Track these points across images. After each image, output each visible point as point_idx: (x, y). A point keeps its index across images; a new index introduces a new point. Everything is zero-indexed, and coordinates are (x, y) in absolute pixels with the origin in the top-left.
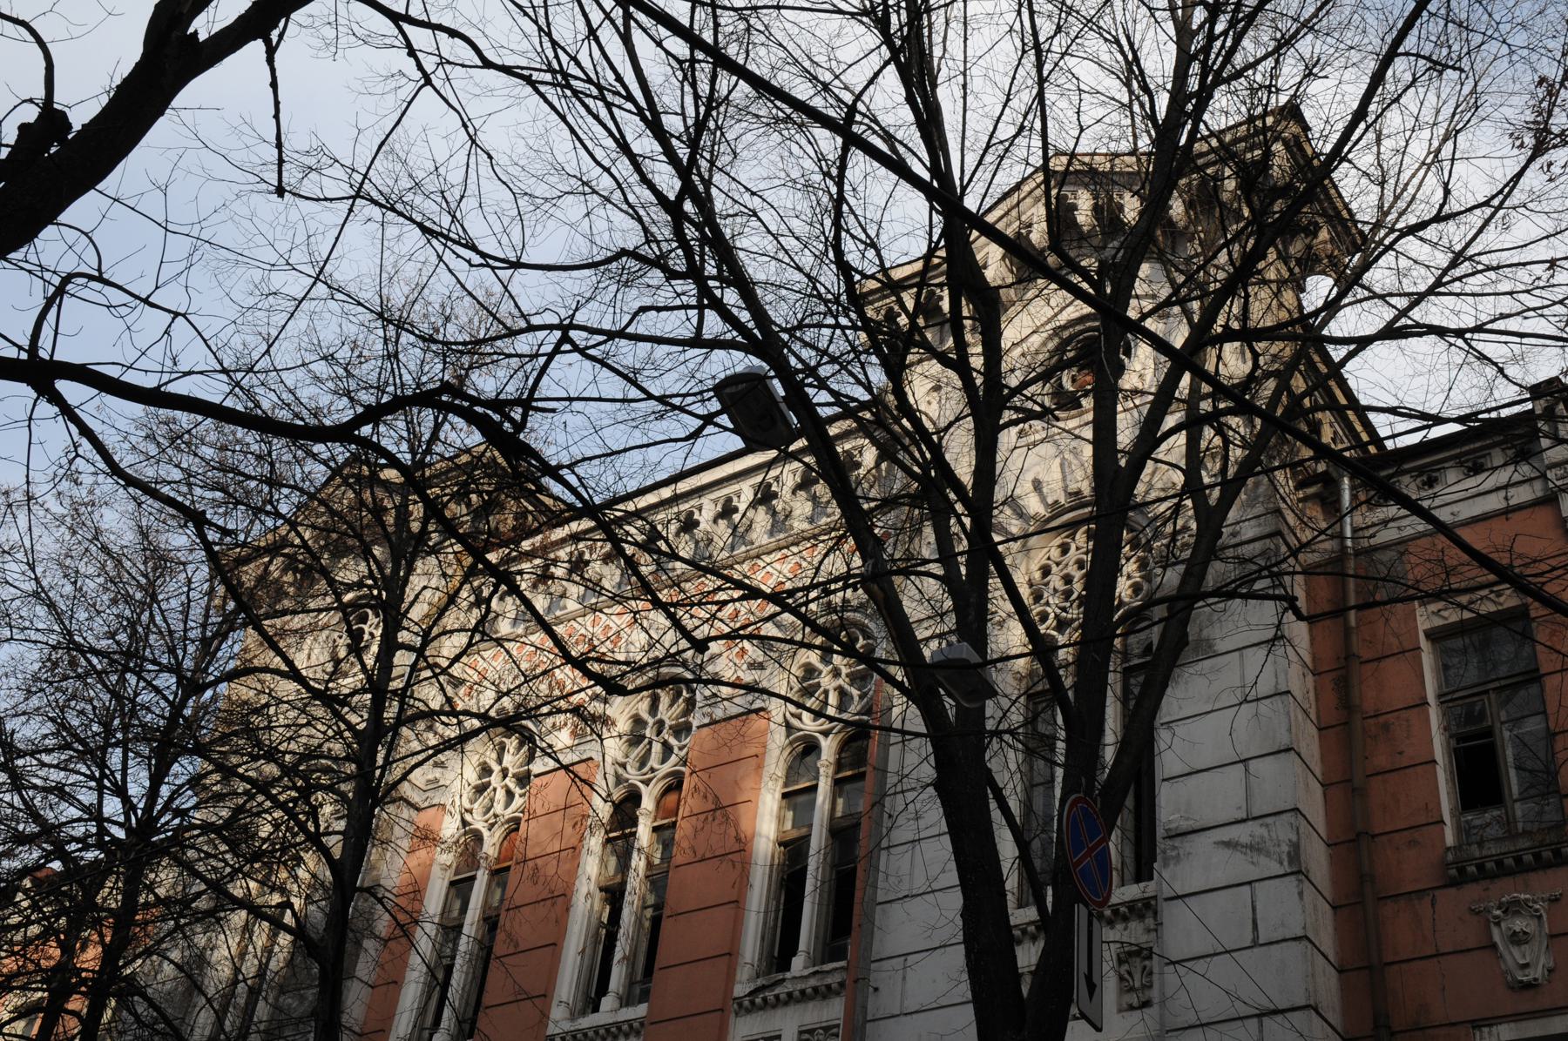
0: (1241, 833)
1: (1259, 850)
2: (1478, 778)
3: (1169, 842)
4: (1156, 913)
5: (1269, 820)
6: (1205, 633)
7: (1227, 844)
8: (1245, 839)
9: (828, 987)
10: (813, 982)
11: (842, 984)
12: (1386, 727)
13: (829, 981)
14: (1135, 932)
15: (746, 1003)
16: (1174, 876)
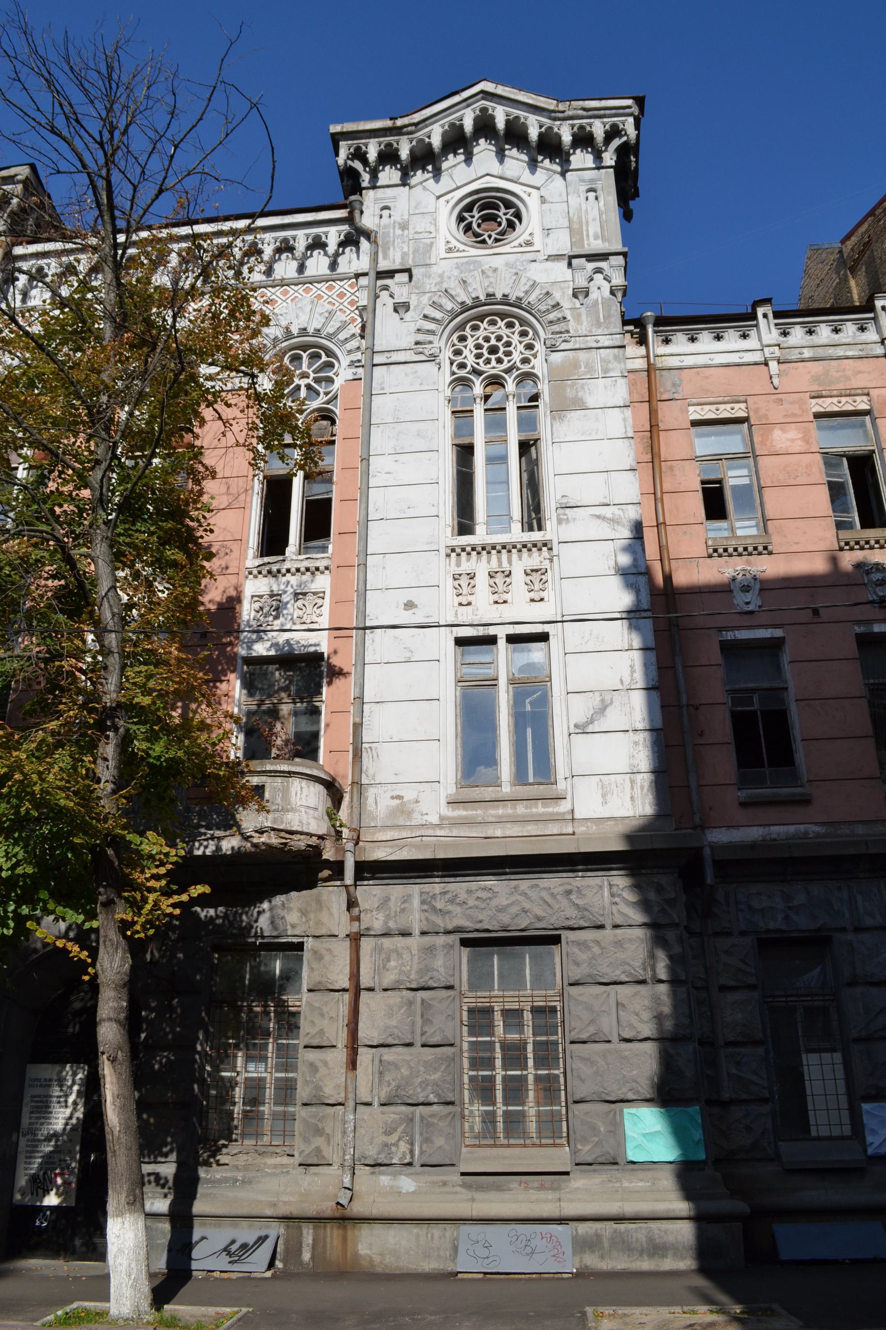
0: (608, 512)
1: (618, 523)
2: (715, 503)
3: (560, 511)
4: (550, 549)
5: (624, 507)
6: (580, 394)
7: (598, 517)
8: (609, 515)
9: (317, 569)
10: (306, 564)
11: (327, 568)
12: (671, 468)
13: (317, 564)
14: (534, 560)
15: (255, 572)
16: (551, 531)
